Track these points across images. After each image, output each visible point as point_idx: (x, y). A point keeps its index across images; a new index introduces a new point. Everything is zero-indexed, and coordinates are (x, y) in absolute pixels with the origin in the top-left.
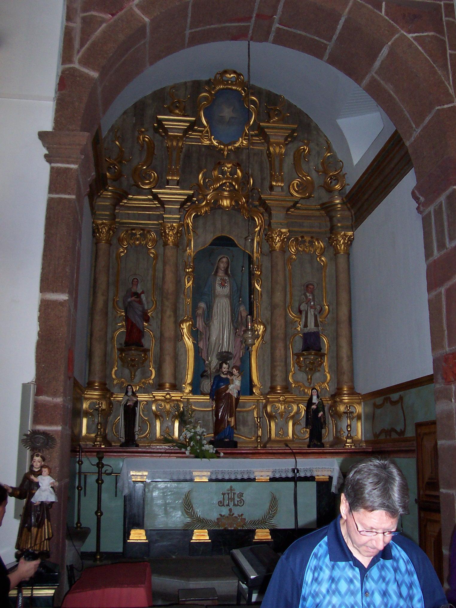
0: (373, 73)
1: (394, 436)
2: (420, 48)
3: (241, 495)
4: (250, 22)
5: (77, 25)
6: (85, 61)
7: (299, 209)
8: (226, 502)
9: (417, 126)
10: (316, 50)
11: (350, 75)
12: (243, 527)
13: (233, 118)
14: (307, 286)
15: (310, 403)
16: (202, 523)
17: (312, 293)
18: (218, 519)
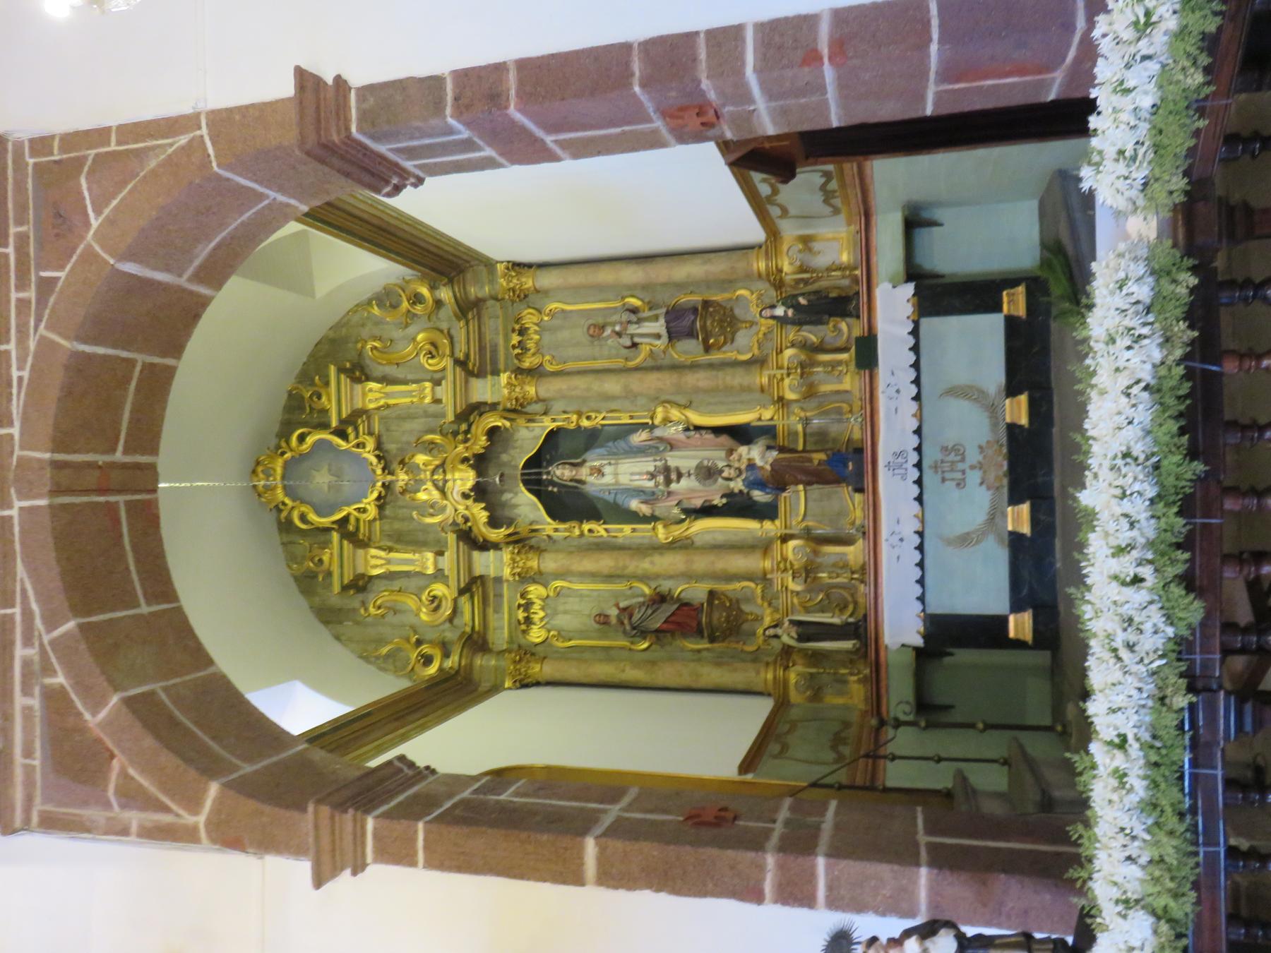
0: (183, 281)
1: (833, 185)
2: (115, 202)
3: (945, 449)
4: (117, 503)
5: (135, 818)
6: (193, 804)
7: (467, 356)
8: (959, 475)
9: (262, 197)
10: (157, 385)
11: (197, 317)
12: (1002, 446)
13: (330, 470)
14: (592, 336)
15: (782, 321)
16: (994, 516)
18: (989, 488)
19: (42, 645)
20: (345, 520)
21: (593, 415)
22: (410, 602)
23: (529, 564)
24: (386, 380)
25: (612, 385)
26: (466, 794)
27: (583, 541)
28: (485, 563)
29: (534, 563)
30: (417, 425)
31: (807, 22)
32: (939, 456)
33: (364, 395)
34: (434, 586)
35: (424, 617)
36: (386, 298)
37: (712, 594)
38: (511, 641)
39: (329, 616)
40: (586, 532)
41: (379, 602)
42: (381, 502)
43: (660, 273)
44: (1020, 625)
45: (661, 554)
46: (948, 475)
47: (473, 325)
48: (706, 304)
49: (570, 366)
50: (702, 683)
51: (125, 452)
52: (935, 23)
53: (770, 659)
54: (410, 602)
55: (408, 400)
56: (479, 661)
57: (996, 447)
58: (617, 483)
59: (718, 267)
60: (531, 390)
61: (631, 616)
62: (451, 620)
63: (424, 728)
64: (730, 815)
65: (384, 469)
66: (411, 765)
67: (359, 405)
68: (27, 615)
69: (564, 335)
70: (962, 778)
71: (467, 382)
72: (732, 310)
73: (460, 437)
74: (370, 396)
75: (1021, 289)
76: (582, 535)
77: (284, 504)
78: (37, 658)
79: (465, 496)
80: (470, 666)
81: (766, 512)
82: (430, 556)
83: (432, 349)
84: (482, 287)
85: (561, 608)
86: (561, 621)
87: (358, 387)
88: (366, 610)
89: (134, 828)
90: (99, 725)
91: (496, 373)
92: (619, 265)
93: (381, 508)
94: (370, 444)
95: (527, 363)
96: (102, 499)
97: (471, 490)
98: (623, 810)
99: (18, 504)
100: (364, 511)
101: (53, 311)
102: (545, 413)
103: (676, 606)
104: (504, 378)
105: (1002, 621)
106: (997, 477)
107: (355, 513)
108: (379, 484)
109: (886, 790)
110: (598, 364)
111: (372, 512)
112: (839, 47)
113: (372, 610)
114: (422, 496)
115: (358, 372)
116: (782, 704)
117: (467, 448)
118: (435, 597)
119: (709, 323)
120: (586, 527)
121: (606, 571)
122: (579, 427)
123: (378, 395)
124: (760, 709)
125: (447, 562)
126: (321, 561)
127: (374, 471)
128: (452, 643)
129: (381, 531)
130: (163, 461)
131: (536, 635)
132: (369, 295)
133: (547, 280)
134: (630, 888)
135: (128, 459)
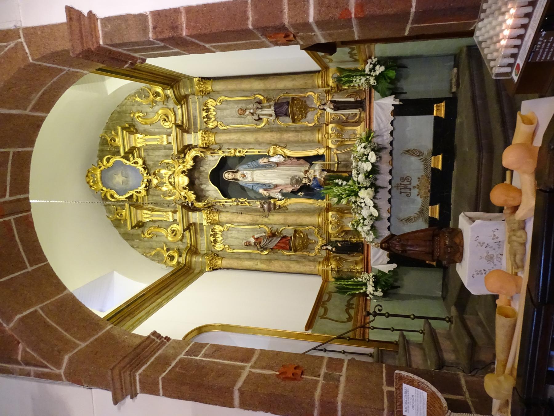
0: (27, 112)
3: (402, 179)
4: (10, 220)
7: (183, 122)
11: (39, 127)
12: (428, 178)
13: (122, 175)
18: (421, 198)
20: (131, 197)
22: (163, 232)
23: (215, 218)
24: (146, 133)
25: (249, 138)
26: (182, 356)
27: (239, 207)
28: (194, 217)
29: (216, 217)
30: (162, 152)
32: (399, 182)
33: (135, 140)
34: (173, 226)
35: (170, 239)
37: (296, 231)
39: (127, 237)
41: (149, 232)
42: (148, 188)
47: (184, 107)
48: (293, 98)
49: (230, 126)
50: (292, 270)
51: (11, 195)
55: (156, 143)
56: (194, 259)
57: (426, 178)
58: (253, 181)
59: (299, 82)
60: (212, 139)
61: (260, 243)
62: (181, 240)
64: (299, 372)
65: (147, 174)
66: (159, 336)
67: (134, 145)
69: (226, 112)
70: (404, 337)
71: (182, 135)
72: (305, 102)
73: (181, 161)
75: (443, 104)
76: (238, 205)
77: (102, 190)
79: (184, 188)
80: (190, 261)
82: (170, 214)
83: (166, 118)
84: (187, 89)
85: (230, 236)
86: (230, 241)
87: (132, 136)
90: (11, 329)
92: (252, 80)
93: (147, 191)
94: (140, 161)
95: (211, 125)
97: (187, 186)
98: (252, 367)
100: (140, 192)
102: (220, 149)
103: (280, 239)
104: (199, 134)
106: (425, 192)
107: (135, 193)
108: (146, 180)
109: (369, 341)
111: (143, 193)
113: (146, 234)
114: (164, 189)
115: (132, 129)
116: (326, 281)
117: (184, 166)
118: (174, 230)
121: (249, 222)
122: (235, 156)
123: (142, 140)
124: (316, 283)
125: (178, 216)
127: (143, 174)
128: (182, 250)
130: (30, 196)
131: (219, 247)
132: (133, 92)
133: (219, 86)
135: (13, 198)
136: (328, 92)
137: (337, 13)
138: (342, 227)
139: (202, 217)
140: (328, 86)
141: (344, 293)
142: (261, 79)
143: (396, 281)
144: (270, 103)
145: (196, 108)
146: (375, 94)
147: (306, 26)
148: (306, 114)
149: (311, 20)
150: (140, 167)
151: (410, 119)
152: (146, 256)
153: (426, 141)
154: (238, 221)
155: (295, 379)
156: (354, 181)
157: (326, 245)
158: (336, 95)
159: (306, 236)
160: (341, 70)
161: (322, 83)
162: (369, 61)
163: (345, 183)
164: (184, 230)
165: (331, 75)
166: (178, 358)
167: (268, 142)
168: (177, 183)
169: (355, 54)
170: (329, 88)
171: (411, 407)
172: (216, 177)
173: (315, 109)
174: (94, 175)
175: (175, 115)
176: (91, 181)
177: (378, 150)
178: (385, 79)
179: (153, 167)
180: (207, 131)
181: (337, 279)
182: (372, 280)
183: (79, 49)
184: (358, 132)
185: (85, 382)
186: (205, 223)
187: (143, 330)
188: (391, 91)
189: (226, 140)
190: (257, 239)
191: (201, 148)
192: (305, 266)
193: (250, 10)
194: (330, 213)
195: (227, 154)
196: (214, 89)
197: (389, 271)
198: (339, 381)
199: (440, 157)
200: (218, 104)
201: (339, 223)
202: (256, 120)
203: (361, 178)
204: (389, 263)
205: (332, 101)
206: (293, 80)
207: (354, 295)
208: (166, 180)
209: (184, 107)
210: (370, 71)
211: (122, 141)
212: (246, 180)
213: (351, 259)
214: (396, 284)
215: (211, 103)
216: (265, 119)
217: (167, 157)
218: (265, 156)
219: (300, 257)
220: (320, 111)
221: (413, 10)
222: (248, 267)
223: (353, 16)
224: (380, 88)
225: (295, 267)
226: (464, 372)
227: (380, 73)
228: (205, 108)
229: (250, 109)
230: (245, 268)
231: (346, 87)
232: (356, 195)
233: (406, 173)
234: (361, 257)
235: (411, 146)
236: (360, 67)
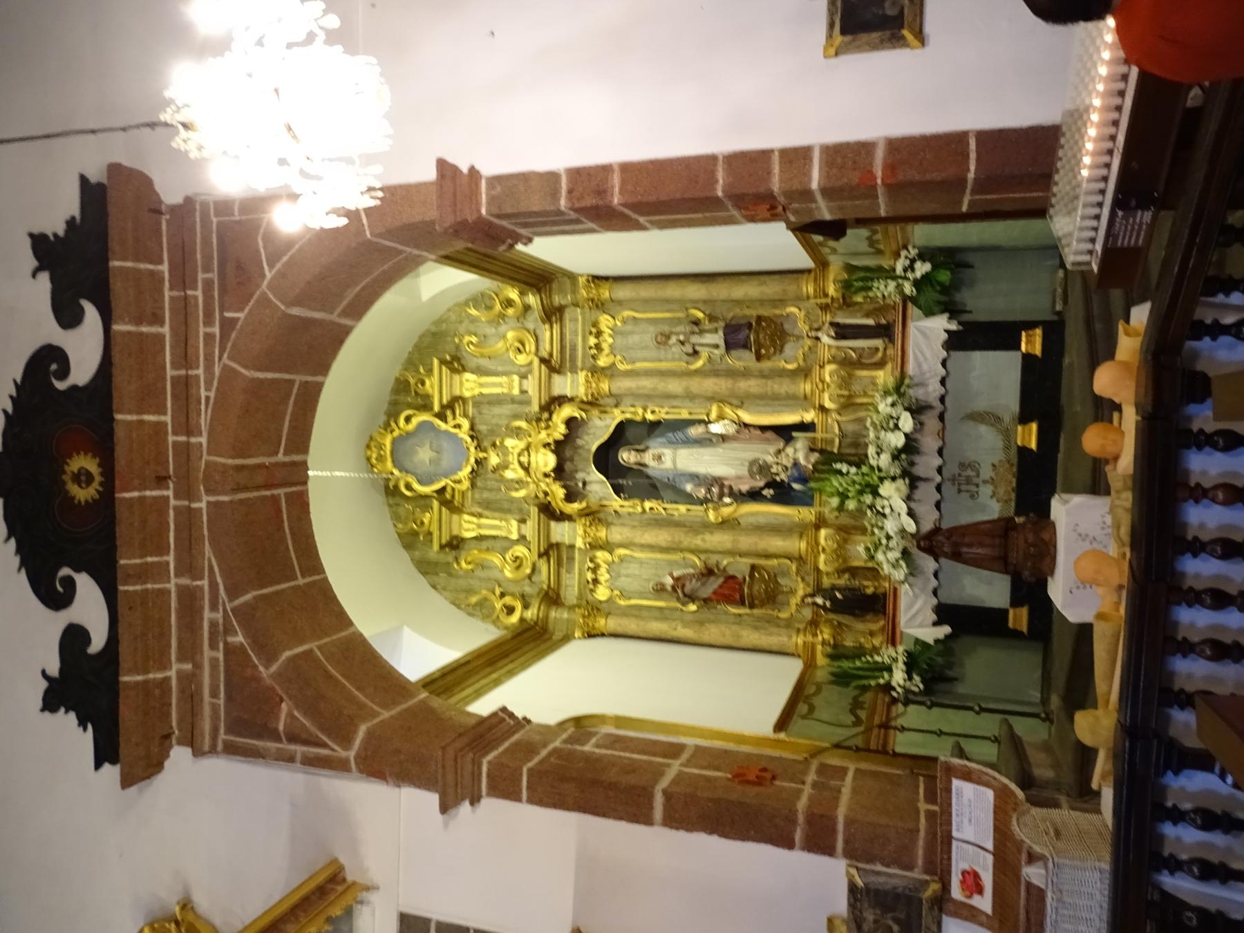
3: (963, 466)
7: (551, 355)
17: (668, 337)
19: (225, 610)
20: (444, 489)
21: (657, 409)
22: (496, 559)
23: (599, 534)
24: (480, 371)
25: (675, 386)
26: (557, 743)
27: (645, 516)
28: (560, 532)
29: (602, 533)
30: (506, 409)
31: (865, 148)
32: (956, 471)
33: (461, 383)
36: (480, 300)
37: (753, 568)
38: (580, 596)
39: (426, 568)
40: (647, 510)
43: (721, 291)
44: (1019, 618)
45: (711, 533)
46: (964, 487)
47: (556, 328)
49: (639, 365)
50: (742, 643)
51: (285, 454)
52: (973, 156)
53: (801, 626)
54: (496, 559)
56: (553, 614)
59: (771, 289)
60: (605, 386)
61: (683, 586)
62: (530, 577)
63: (511, 674)
64: (768, 775)
66: (511, 715)
68: (213, 585)
69: (634, 339)
71: (550, 377)
73: (543, 425)
74: (467, 385)
75: (1038, 332)
77: (392, 473)
78: (221, 621)
81: (804, 500)
82: (514, 523)
86: (623, 582)
87: (456, 377)
88: (458, 564)
89: (299, 757)
90: (271, 676)
91: (574, 370)
92: (683, 282)
94: (466, 424)
95: (602, 362)
96: (268, 493)
98: (682, 765)
99: (205, 498)
100: (459, 482)
101: (234, 345)
102: (616, 406)
104: (582, 376)
105: (1006, 612)
108: (472, 460)
109: (895, 755)
110: (664, 365)
111: (466, 484)
112: (890, 168)
113: (463, 564)
114: (509, 474)
115: (456, 364)
116: (810, 665)
117: (548, 435)
118: (517, 558)
119: (761, 336)
120: (648, 505)
121: (664, 544)
122: (645, 419)
124: (792, 669)
125: (530, 529)
126: (422, 523)
128: (531, 596)
129: (473, 498)
130: (311, 459)
131: (602, 593)
132: (467, 296)
133: (623, 292)
134: (688, 830)
135: (287, 459)
136: (825, 308)
137: (855, 177)
138: (845, 560)
139: (575, 530)
140: (826, 295)
141: (847, 685)
142: (702, 282)
143: (950, 666)
144: (715, 325)
145: (576, 331)
146: (913, 310)
147: (807, 195)
148: (782, 347)
149: (814, 185)
150: (464, 434)
151: (977, 356)
152: (458, 607)
153: (1009, 398)
154: (643, 541)
155: (760, 784)
156: (872, 468)
157: (813, 595)
158: (839, 313)
159: (774, 578)
160: (850, 268)
161: (815, 290)
162: (903, 253)
163: (853, 470)
164: (540, 556)
165: (831, 277)
166: (551, 747)
167: (710, 394)
168: (533, 465)
169: (878, 241)
170: (829, 301)
171: (966, 821)
172: (605, 459)
173: (799, 338)
174: (380, 447)
175: (537, 341)
176: (374, 456)
177: (917, 410)
178: (932, 286)
179: (486, 436)
180: (595, 371)
181: (833, 657)
182: (901, 659)
183: (449, 220)
184: (880, 381)
185: (391, 775)
186: (579, 543)
187: (483, 707)
188: (943, 307)
189: (630, 389)
190: (677, 580)
191: (582, 402)
192: (771, 634)
193: (720, 169)
194: (823, 532)
195: (628, 416)
196: (613, 296)
197: (937, 641)
198: (839, 791)
199: (1034, 426)
200: (619, 324)
201: (840, 552)
202: (688, 354)
203: (885, 460)
204: (935, 624)
205: (832, 324)
206: (761, 284)
207: (865, 689)
208: (513, 459)
209: (556, 328)
210: (905, 270)
211: (438, 385)
212: (663, 466)
213: (860, 626)
214: (950, 673)
215: (605, 321)
216: (704, 352)
217: (517, 417)
218: (701, 422)
219: (759, 619)
220: (809, 342)
221: (971, 175)
222: (658, 634)
223: (879, 181)
224: (922, 301)
225: (751, 637)
226: (1068, 795)
227: (923, 277)
228: (594, 330)
229: (678, 334)
230: (651, 635)
231: (859, 299)
232: (875, 493)
233: (971, 456)
234: (882, 623)
235: (981, 405)
236: (886, 263)
